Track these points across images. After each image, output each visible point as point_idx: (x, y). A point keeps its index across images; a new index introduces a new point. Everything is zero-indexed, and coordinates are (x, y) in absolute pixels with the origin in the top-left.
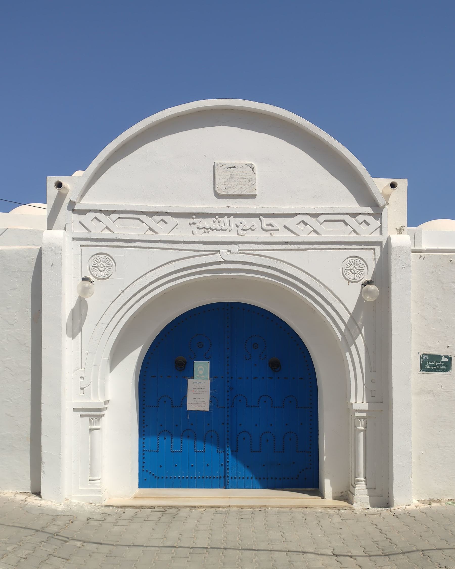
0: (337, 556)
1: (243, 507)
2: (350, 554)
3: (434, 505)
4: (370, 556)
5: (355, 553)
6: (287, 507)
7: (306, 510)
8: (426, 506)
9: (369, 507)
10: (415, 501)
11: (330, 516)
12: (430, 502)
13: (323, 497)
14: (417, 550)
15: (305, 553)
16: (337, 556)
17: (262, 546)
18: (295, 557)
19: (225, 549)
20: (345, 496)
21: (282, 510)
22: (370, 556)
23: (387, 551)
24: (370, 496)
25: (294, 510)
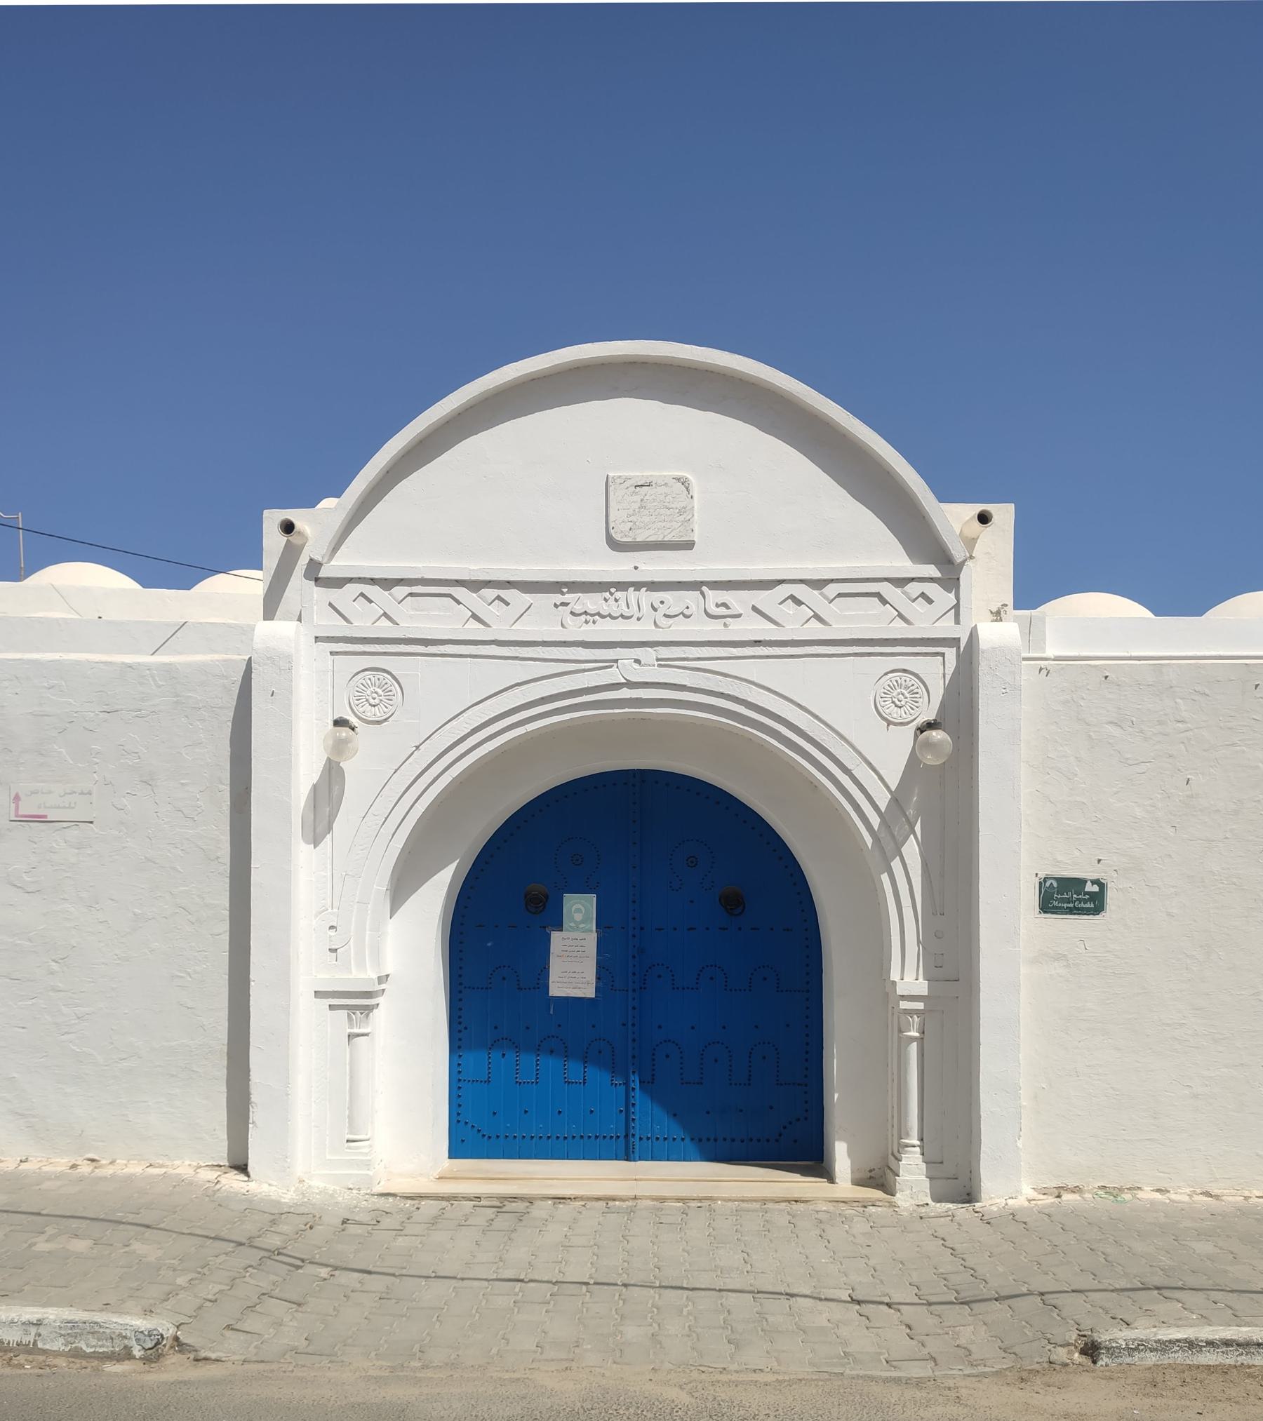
0: (859, 1303)
1: (663, 1199)
2: (886, 1300)
3: (1067, 1197)
4: (930, 1304)
5: (897, 1297)
6: (756, 1200)
7: (795, 1206)
8: (1051, 1200)
9: (929, 1201)
10: (1027, 1191)
11: (846, 1219)
12: (1059, 1192)
13: (831, 1180)
14: (1030, 1293)
15: (792, 1295)
16: (859, 1303)
17: (704, 1280)
18: (771, 1304)
19: (625, 1285)
20: (879, 1178)
21: (744, 1205)
22: (930, 1304)
23: (966, 1295)
24: (931, 1178)
25: (770, 1205)
